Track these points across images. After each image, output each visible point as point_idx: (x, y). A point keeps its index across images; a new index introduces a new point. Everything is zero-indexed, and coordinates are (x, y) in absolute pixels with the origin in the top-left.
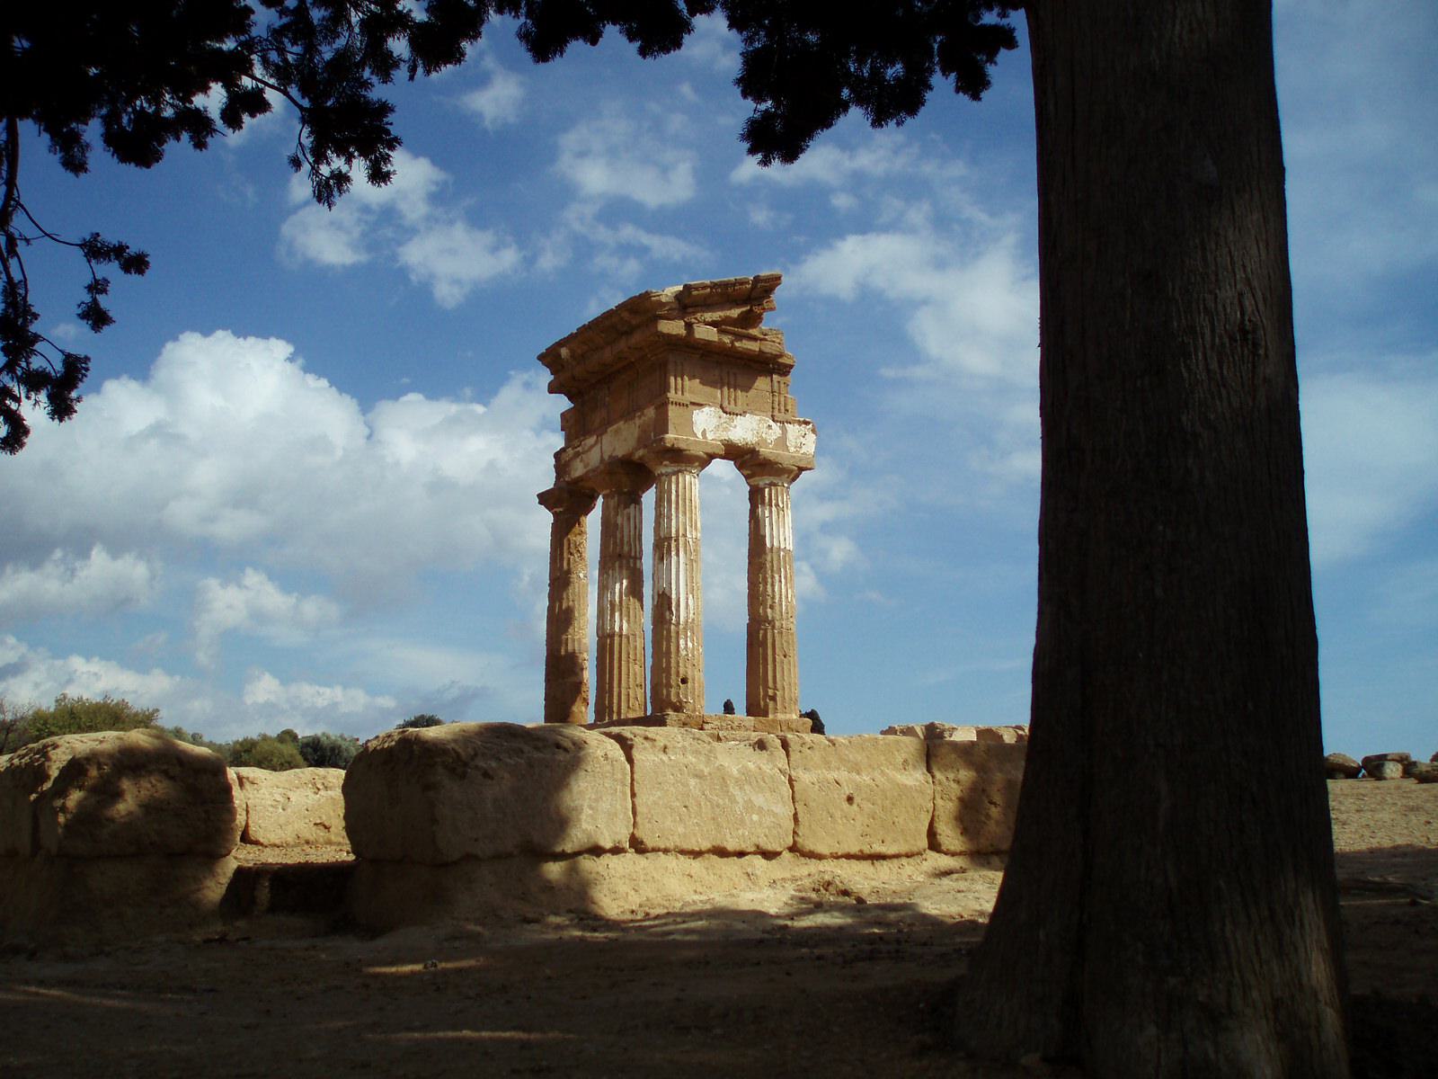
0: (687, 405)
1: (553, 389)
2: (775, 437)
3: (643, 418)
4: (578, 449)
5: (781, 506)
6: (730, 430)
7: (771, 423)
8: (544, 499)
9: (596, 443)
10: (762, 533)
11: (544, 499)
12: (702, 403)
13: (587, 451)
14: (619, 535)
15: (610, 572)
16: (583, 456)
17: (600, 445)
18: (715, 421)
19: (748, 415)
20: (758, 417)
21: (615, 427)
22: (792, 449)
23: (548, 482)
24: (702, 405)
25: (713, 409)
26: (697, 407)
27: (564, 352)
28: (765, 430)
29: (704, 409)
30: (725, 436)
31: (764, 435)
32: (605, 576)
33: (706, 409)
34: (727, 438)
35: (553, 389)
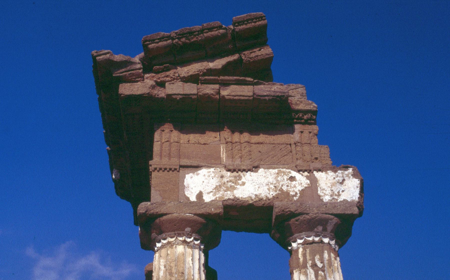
0: (175, 169)
2: (300, 188)
5: (320, 265)
6: (235, 188)
7: (294, 174)
12: (195, 163)
18: (215, 182)
19: (261, 170)
20: (276, 171)
22: (326, 199)
24: (197, 167)
25: (212, 170)
26: (186, 170)
28: (286, 182)
29: (199, 172)
30: (229, 195)
31: (285, 188)
33: (203, 171)
34: (232, 197)
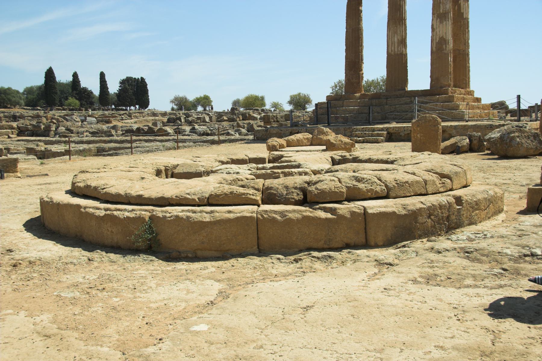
10: (462, 11)
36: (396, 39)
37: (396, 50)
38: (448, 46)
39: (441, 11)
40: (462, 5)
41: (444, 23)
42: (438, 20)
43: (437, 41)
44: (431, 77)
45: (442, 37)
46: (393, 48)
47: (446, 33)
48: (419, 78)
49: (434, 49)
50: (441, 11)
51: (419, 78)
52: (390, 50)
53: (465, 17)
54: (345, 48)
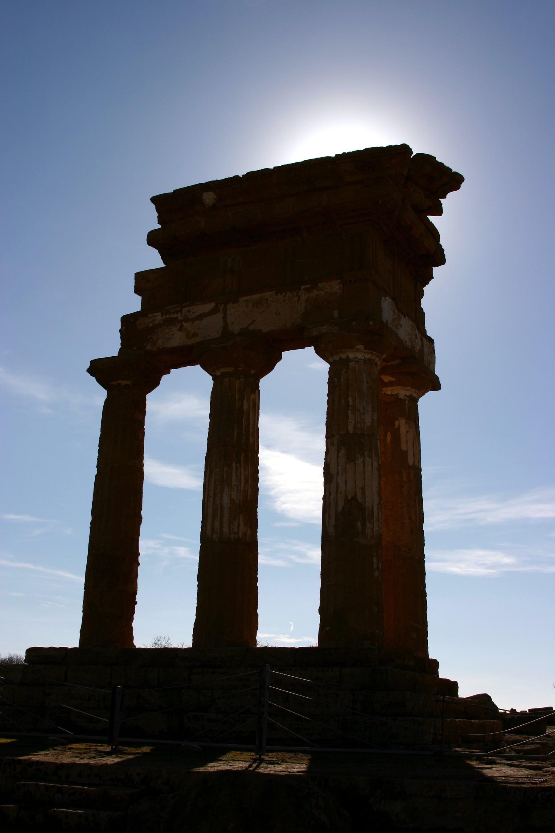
1: (153, 239)
3: (315, 292)
4: (175, 316)
8: (99, 369)
9: (214, 311)
10: (404, 447)
11: (99, 369)
13: (194, 320)
14: (244, 424)
15: (234, 465)
16: (185, 325)
17: (220, 315)
21: (256, 297)
23: (111, 346)
27: (209, 198)
32: (226, 469)
35: (153, 239)
36: (226, 501)
37: (226, 529)
38: (368, 525)
39: (351, 429)
40: (403, 431)
41: (359, 461)
42: (343, 451)
43: (340, 509)
44: (321, 611)
45: (354, 498)
46: (217, 524)
47: (363, 489)
48: (289, 614)
49: (331, 530)
50: (351, 429)
51: (289, 614)
52: (209, 528)
53: (411, 462)
54: (90, 519)
